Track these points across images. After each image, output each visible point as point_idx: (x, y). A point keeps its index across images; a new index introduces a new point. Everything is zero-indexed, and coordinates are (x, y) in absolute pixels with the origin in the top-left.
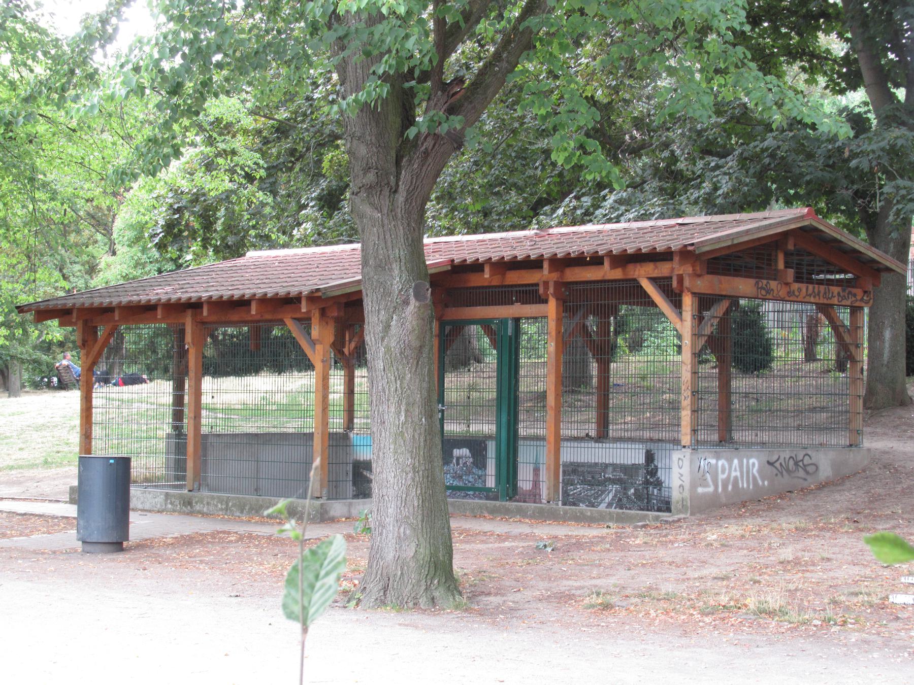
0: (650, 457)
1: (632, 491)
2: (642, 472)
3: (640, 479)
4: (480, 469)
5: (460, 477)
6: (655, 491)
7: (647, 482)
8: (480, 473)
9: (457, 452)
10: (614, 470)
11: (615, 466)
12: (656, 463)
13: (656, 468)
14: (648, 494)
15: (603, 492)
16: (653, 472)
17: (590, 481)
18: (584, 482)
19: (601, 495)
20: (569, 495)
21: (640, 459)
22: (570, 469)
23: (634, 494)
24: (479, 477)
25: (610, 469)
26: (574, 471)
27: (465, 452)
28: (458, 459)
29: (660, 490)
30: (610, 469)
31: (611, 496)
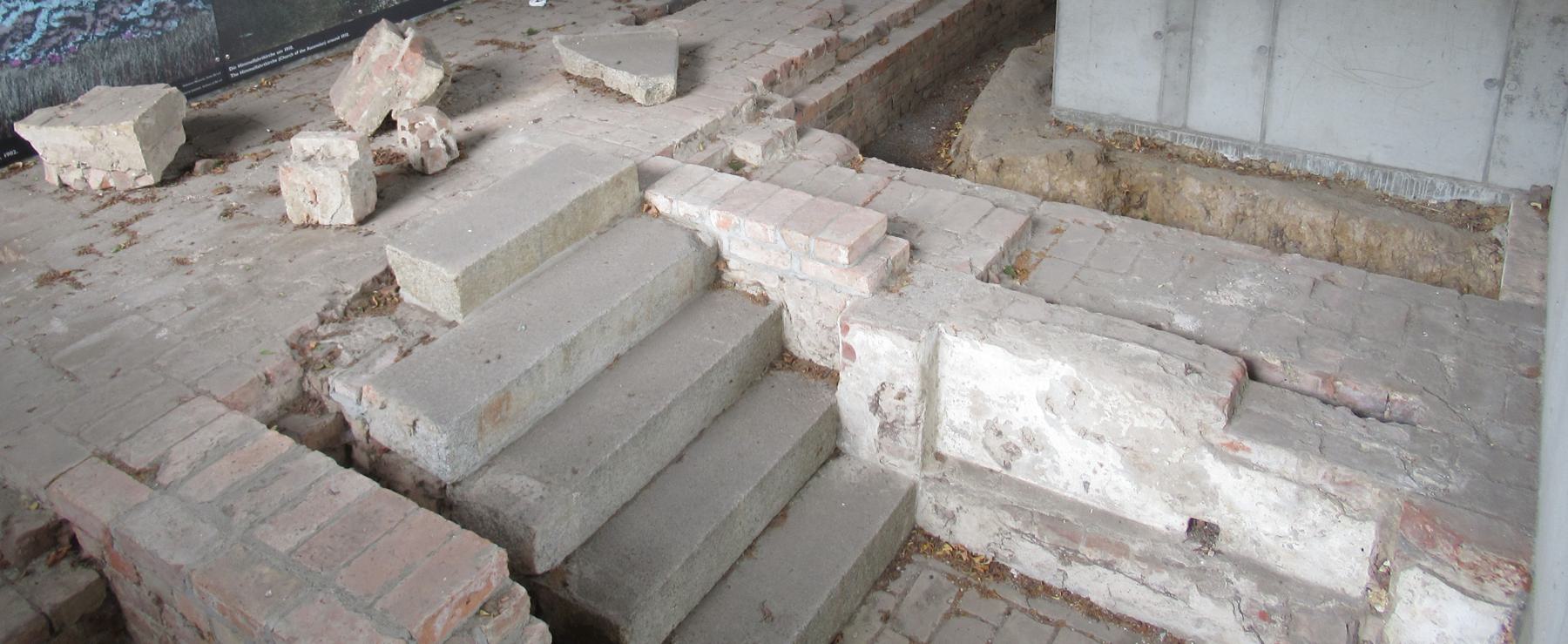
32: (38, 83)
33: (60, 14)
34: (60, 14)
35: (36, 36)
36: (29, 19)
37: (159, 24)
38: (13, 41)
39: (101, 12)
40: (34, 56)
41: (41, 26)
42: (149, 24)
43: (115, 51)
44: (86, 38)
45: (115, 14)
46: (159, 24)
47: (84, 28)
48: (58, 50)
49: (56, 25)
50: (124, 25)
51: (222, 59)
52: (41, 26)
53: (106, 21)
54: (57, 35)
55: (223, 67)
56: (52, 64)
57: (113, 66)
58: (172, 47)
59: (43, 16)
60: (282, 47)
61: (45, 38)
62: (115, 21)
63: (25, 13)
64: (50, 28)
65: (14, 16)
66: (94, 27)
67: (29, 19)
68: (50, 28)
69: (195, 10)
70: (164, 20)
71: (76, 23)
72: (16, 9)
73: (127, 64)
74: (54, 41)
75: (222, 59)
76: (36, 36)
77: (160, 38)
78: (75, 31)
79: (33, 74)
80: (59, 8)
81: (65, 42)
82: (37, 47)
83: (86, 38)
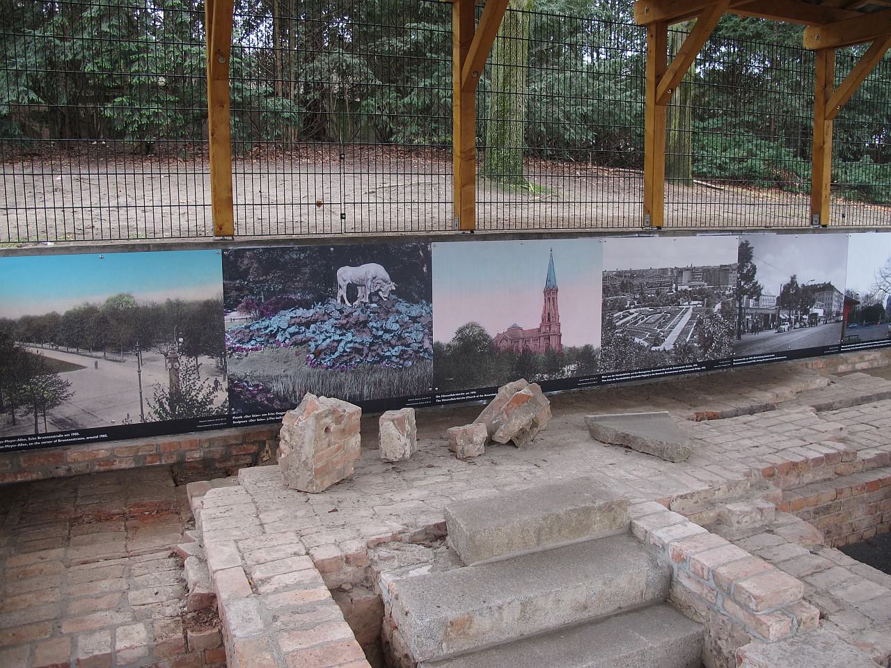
0: (745, 253)
1: (718, 306)
2: (734, 276)
3: (731, 287)
4: (417, 302)
5: (362, 325)
6: (752, 302)
7: (740, 292)
8: (415, 310)
9: (346, 274)
10: (693, 278)
11: (693, 271)
12: (754, 261)
13: (754, 268)
14: (740, 308)
15: (673, 315)
16: (749, 276)
17: (652, 299)
18: (643, 301)
19: (670, 319)
20: (615, 328)
21: (732, 259)
22: (618, 283)
23: (721, 311)
24: (414, 320)
25: (686, 276)
26: (624, 287)
27: (373, 271)
28: (352, 290)
29: (757, 300)
30: (686, 276)
31: (687, 316)
32: (333, 379)
33: (351, 345)
34: (351, 345)
35: (337, 354)
36: (335, 344)
37: (401, 362)
38: (325, 354)
39: (372, 348)
40: (334, 365)
41: (340, 349)
42: (395, 361)
43: (375, 372)
44: (362, 361)
45: (379, 351)
46: (401, 362)
47: (362, 356)
48: (346, 364)
49: (348, 350)
50: (382, 358)
51: (434, 389)
52: (340, 349)
53: (374, 354)
54: (347, 356)
55: (433, 395)
56: (342, 371)
57: (373, 379)
58: (406, 376)
59: (342, 344)
60: (469, 391)
61: (341, 356)
62: (378, 354)
63: (334, 340)
64: (345, 351)
65: (328, 341)
66: (367, 356)
67: (335, 344)
68: (345, 351)
69: (423, 358)
70: (405, 360)
71: (358, 351)
72: (330, 337)
73: (380, 380)
74: (345, 358)
75: (434, 389)
76: (337, 354)
77: (401, 369)
78: (357, 356)
79: (331, 374)
80: (351, 342)
81: (351, 360)
82: (336, 360)
83: (362, 361)
